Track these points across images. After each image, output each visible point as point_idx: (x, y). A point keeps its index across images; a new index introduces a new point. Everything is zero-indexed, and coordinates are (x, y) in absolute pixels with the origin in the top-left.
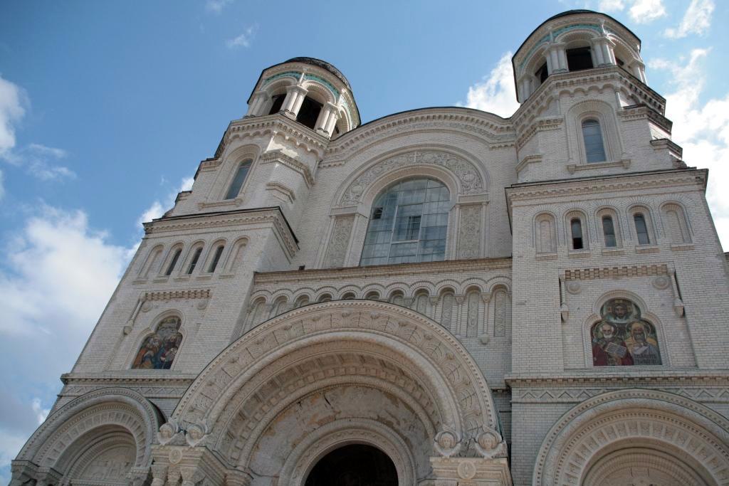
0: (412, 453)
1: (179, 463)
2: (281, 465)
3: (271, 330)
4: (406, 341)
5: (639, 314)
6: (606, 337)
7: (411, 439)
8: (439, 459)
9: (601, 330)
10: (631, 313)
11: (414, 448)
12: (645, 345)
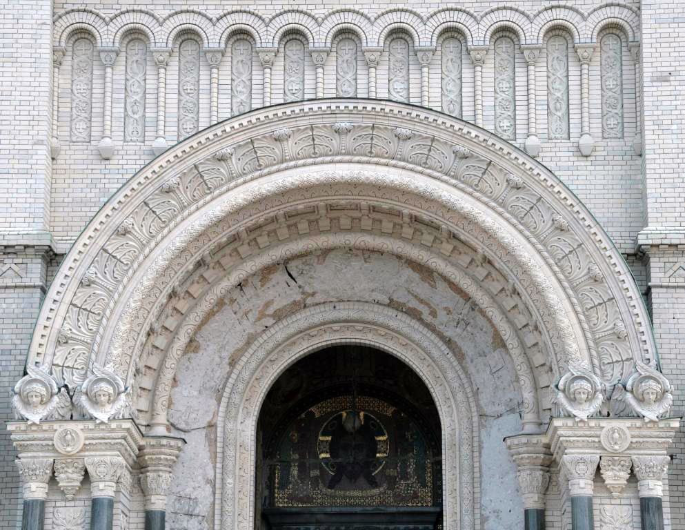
0: (464, 368)
1: (81, 451)
2: (214, 402)
3: (191, 162)
4: (473, 188)
7: (460, 343)
8: (570, 423)
11: (468, 359)
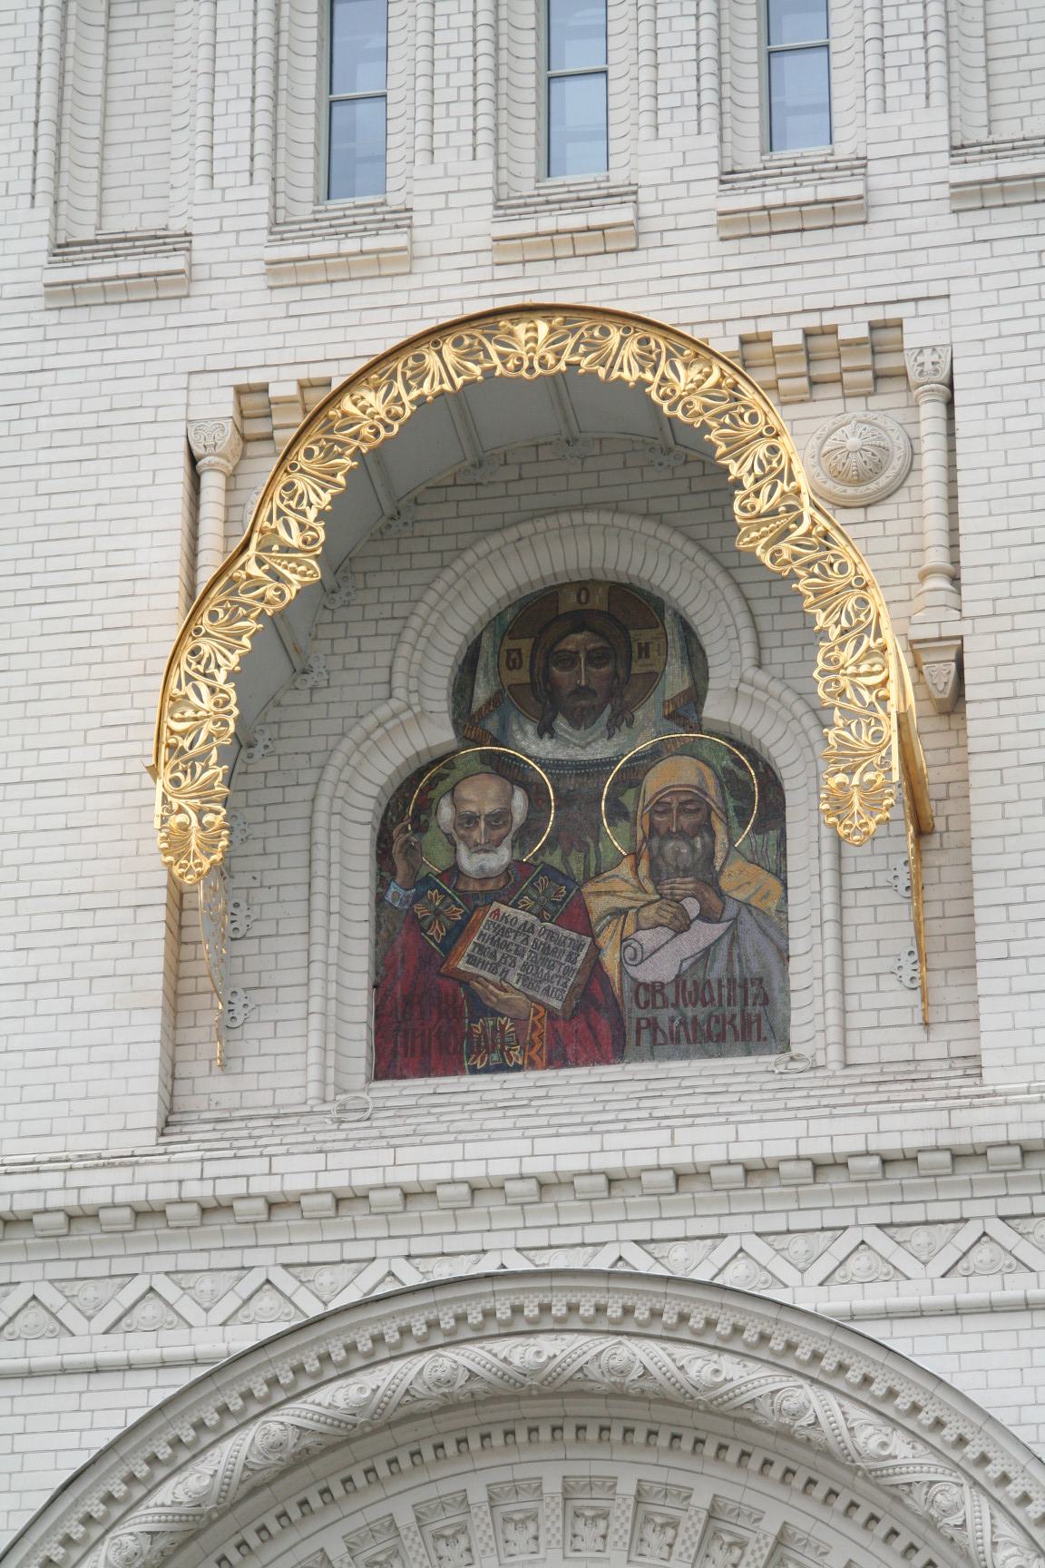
5: (696, 696)
6: (470, 862)
9: (446, 812)
10: (653, 678)
12: (705, 916)
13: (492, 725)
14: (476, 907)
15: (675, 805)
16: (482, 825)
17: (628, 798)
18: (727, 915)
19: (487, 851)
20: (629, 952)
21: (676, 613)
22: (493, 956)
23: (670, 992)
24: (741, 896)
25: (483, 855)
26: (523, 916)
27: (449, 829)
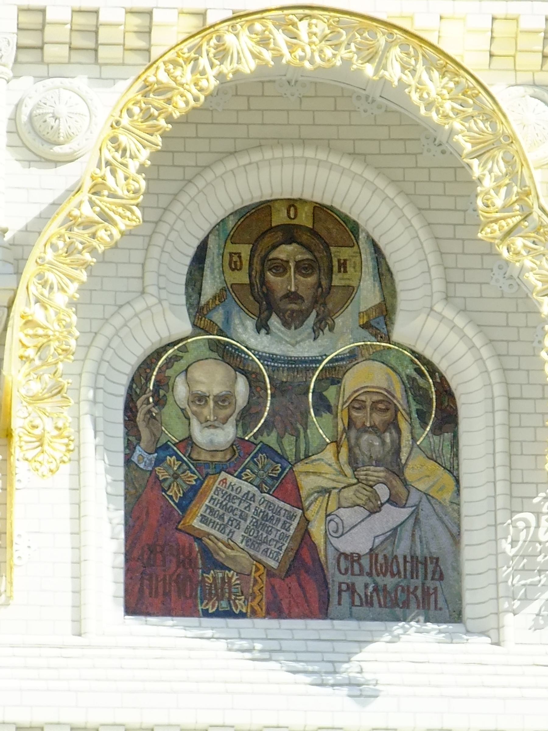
6: (201, 435)
9: (181, 390)
10: (350, 291)
13: (218, 317)
14: (207, 475)
15: (368, 403)
16: (211, 403)
17: (330, 393)
18: (411, 502)
19: (215, 427)
20: (332, 525)
21: (368, 236)
22: (221, 517)
23: (365, 562)
24: (422, 486)
25: (212, 430)
26: (246, 487)
27: (183, 404)
